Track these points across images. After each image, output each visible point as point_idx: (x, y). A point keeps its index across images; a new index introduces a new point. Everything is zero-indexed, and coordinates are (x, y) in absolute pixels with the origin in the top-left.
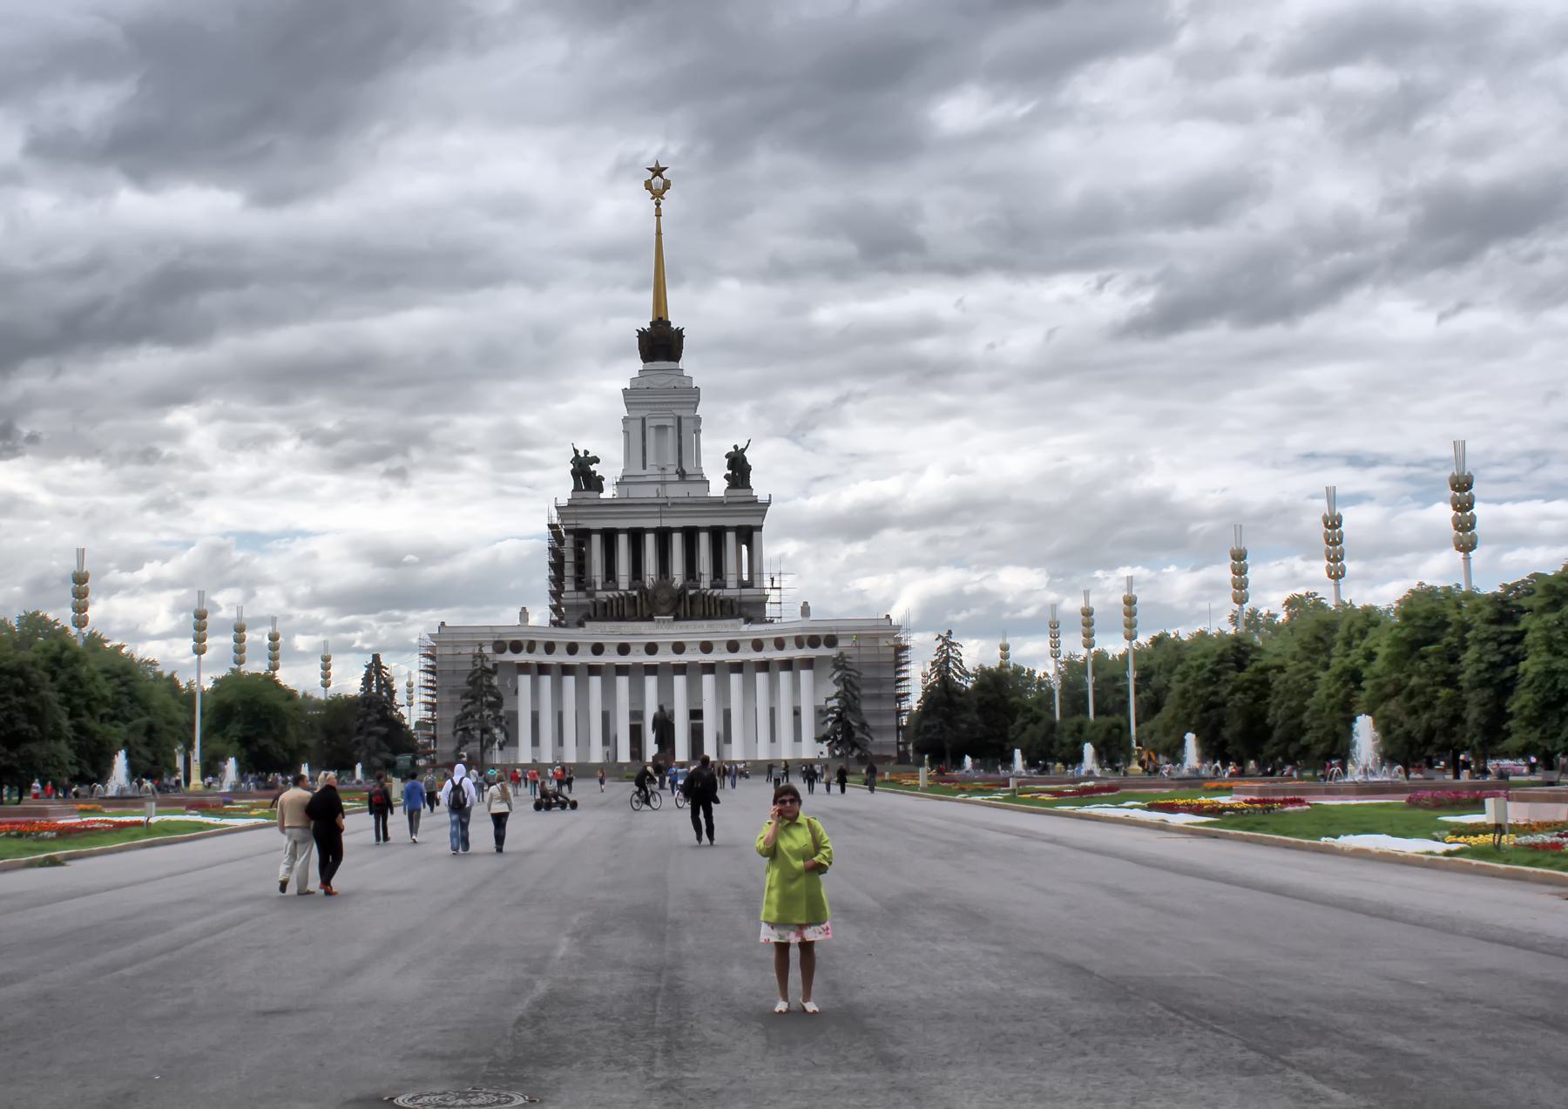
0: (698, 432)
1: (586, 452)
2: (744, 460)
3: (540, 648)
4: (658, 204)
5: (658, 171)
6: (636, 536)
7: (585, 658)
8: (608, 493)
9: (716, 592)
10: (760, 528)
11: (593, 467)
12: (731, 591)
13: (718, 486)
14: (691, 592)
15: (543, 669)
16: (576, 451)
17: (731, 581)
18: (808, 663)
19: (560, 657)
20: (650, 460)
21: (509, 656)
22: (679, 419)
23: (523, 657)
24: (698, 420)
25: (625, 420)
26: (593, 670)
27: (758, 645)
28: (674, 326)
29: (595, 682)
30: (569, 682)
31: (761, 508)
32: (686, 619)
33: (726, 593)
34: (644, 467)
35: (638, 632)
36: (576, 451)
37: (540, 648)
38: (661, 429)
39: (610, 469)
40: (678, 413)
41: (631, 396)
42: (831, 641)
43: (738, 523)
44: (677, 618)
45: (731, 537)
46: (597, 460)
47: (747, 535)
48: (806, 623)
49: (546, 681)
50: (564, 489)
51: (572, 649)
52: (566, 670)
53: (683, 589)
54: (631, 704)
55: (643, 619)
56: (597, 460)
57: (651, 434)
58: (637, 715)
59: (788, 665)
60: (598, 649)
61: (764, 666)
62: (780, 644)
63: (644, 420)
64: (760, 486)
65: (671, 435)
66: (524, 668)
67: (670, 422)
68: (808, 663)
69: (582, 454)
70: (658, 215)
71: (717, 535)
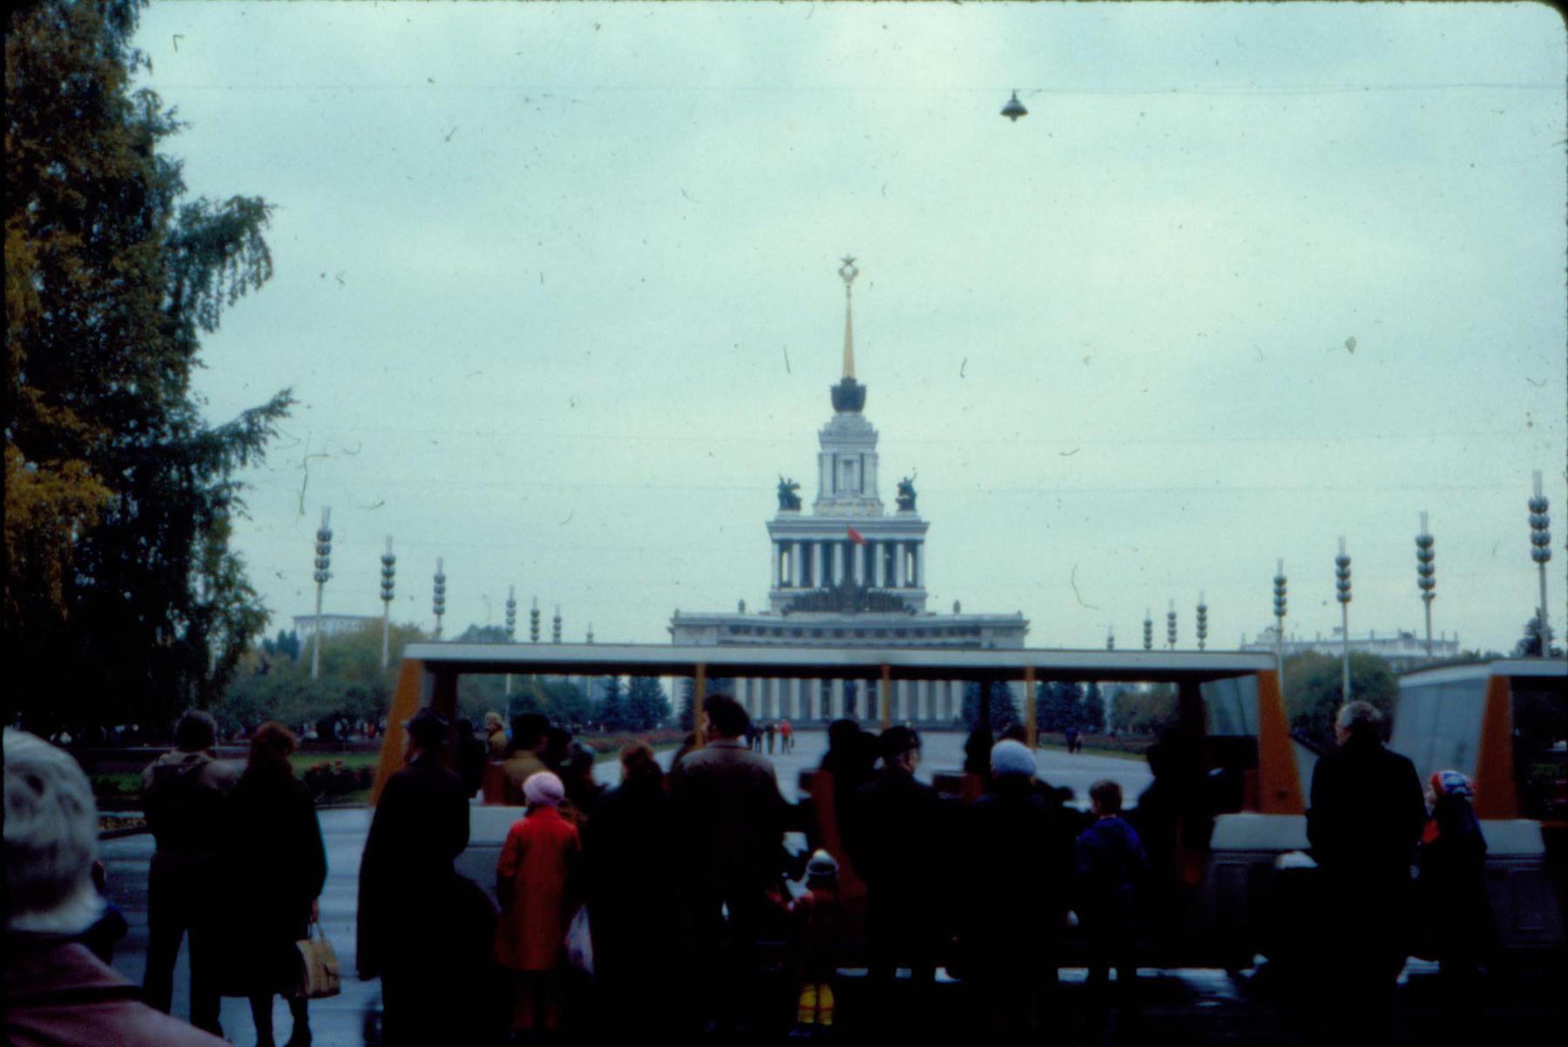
0: (875, 465)
5: (849, 262)
6: (828, 546)
8: (807, 510)
9: (890, 590)
10: (922, 542)
12: (900, 589)
13: (891, 509)
14: (870, 590)
17: (900, 581)
22: (862, 456)
24: (875, 457)
25: (821, 457)
28: (860, 381)
31: (922, 527)
33: (894, 591)
38: (848, 463)
39: (808, 496)
40: (862, 450)
41: (827, 437)
43: (906, 541)
45: (900, 549)
46: (797, 486)
47: (913, 547)
48: (957, 618)
50: (771, 508)
53: (865, 587)
56: (797, 486)
57: (841, 468)
64: (924, 509)
65: (856, 467)
70: (849, 295)
71: (890, 546)
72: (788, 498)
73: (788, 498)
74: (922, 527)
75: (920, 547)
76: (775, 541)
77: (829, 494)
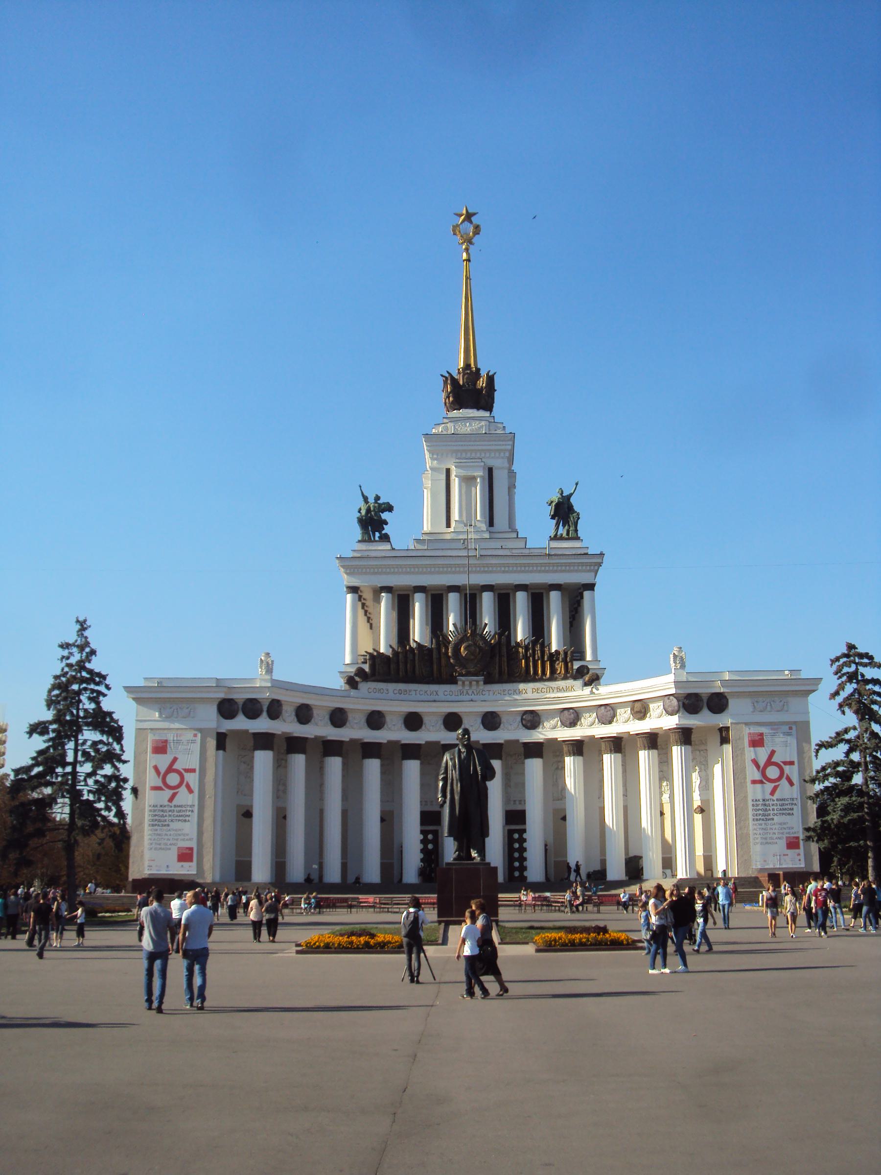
0: (512, 487)
1: (377, 498)
2: (571, 509)
3: (288, 712)
4: (467, 250)
7: (356, 731)
10: (591, 587)
11: (385, 516)
15: (294, 744)
16: (366, 499)
18: (685, 735)
19: (320, 729)
20: (455, 515)
21: (241, 723)
22: (490, 471)
23: (262, 724)
24: (512, 474)
26: (370, 750)
27: (607, 714)
29: (373, 767)
30: (335, 764)
31: (595, 562)
32: (501, 681)
34: (448, 525)
35: (432, 701)
36: (366, 499)
37: (288, 712)
40: (491, 463)
42: (718, 703)
44: (489, 681)
45: (555, 598)
46: (390, 508)
49: (299, 761)
51: (338, 718)
52: (331, 748)
54: (423, 802)
55: (440, 681)
56: (390, 508)
58: (430, 818)
59: (652, 740)
60: (375, 720)
61: (617, 744)
62: (640, 709)
63: (448, 471)
64: (592, 534)
66: (264, 741)
67: (480, 473)
68: (685, 735)
69: (371, 500)
72: (373, 522)
73: (373, 522)
74: (595, 562)
75: (586, 594)
76: (354, 590)
77: (442, 528)
